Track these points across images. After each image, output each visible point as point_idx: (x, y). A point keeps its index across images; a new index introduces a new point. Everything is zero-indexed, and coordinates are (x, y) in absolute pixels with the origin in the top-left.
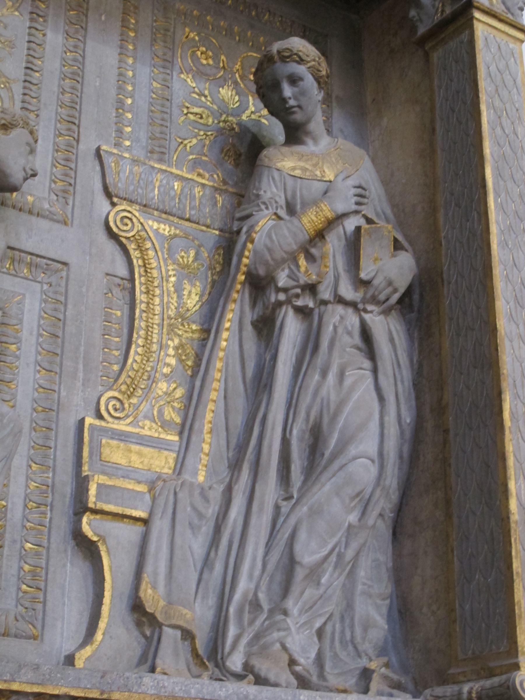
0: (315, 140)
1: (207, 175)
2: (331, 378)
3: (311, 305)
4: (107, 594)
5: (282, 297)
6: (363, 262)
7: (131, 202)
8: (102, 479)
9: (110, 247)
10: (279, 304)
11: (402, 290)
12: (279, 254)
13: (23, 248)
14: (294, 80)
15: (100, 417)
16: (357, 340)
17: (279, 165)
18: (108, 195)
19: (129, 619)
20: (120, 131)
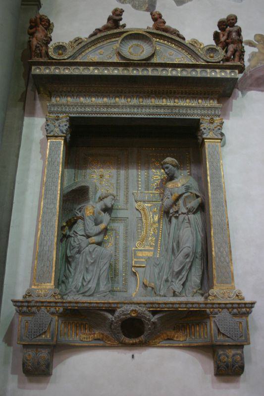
0: (177, 178)
1: (159, 190)
2: (181, 231)
3: (177, 215)
4: (138, 282)
5: (171, 215)
6: (187, 204)
7: (141, 201)
8: (135, 260)
9: (137, 212)
10: (171, 217)
11: (196, 208)
12: (169, 206)
13: (119, 217)
14: (167, 168)
15: (136, 247)
16: (187, 221)
17: (168, 186)
18: (136, 201)
19: (143, 286)
20: (138, 187)
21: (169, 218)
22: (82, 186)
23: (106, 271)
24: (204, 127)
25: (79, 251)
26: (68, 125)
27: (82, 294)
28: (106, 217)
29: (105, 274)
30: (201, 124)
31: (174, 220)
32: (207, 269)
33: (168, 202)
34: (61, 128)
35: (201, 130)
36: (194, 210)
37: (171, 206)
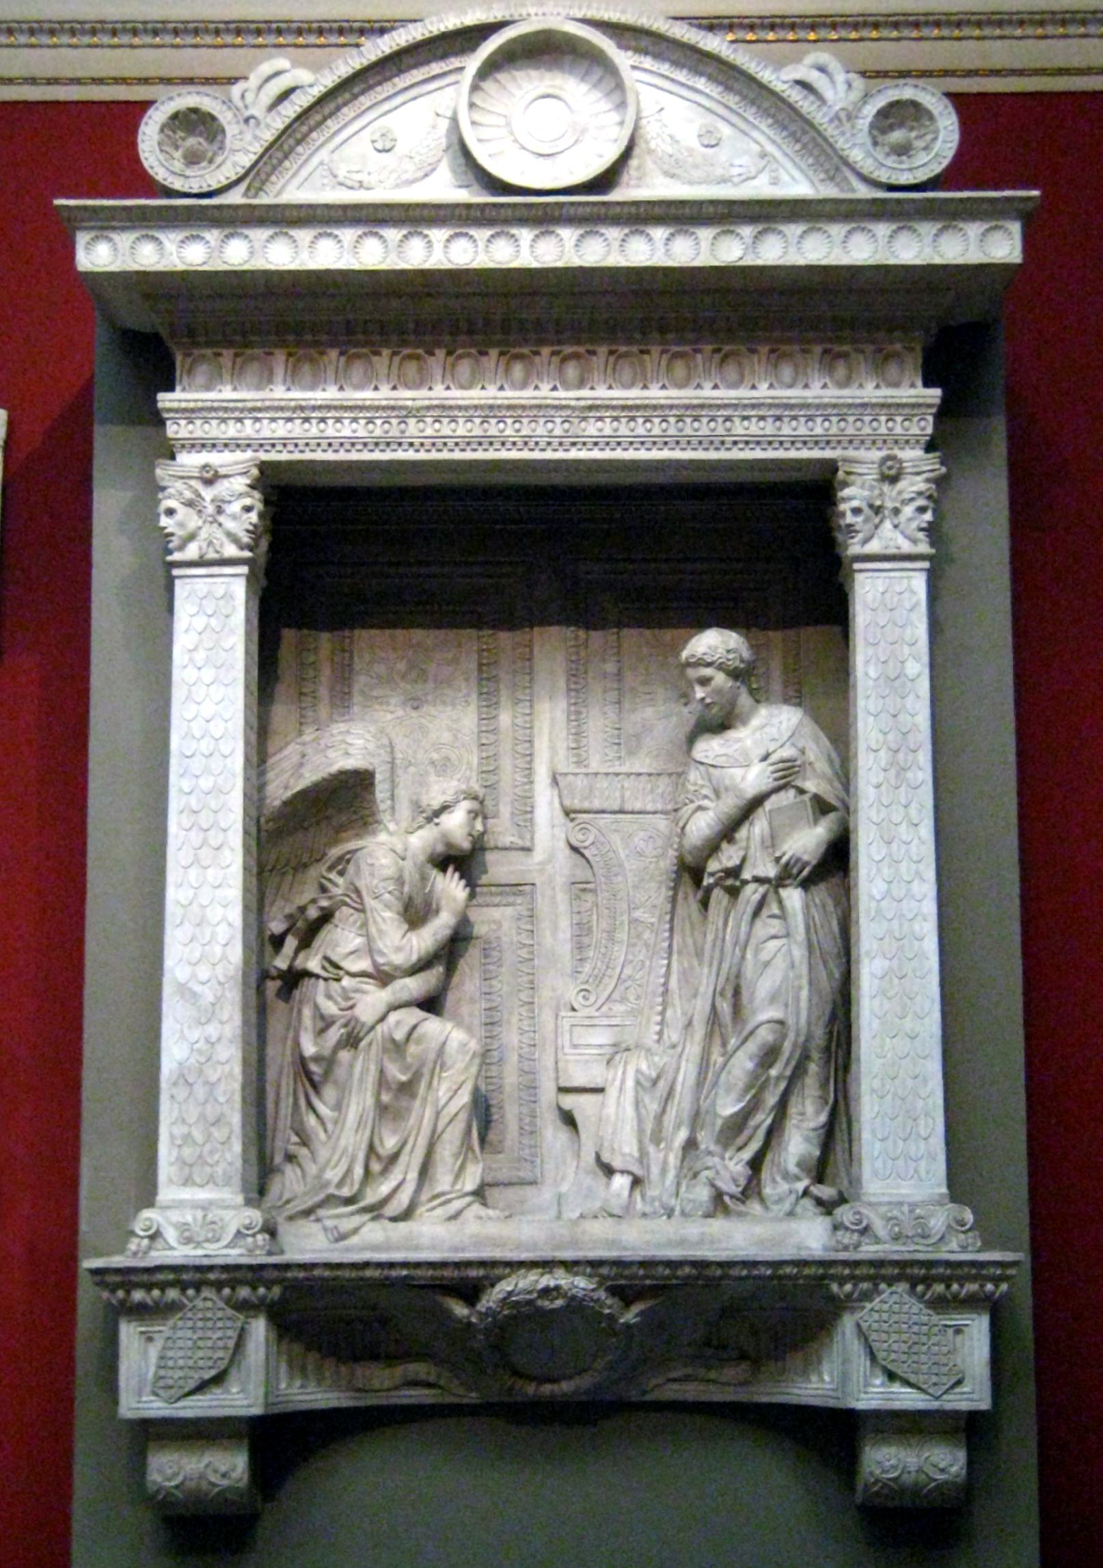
21: (700, 894)
22: (342, 773)
23: (463, 1116)
24: (855, 503)
25: (349, 1035)
26: (259, 506)
27: (366, 1210)
28: (451, 888)
29: (459, 1126)
30: (845, 484)
31: (719, 897)
32: (846, 1097)
33: (701, 826)
34: (230, 525)
35: (843, 514)
36: (805, 873)
37: (712, 848)
